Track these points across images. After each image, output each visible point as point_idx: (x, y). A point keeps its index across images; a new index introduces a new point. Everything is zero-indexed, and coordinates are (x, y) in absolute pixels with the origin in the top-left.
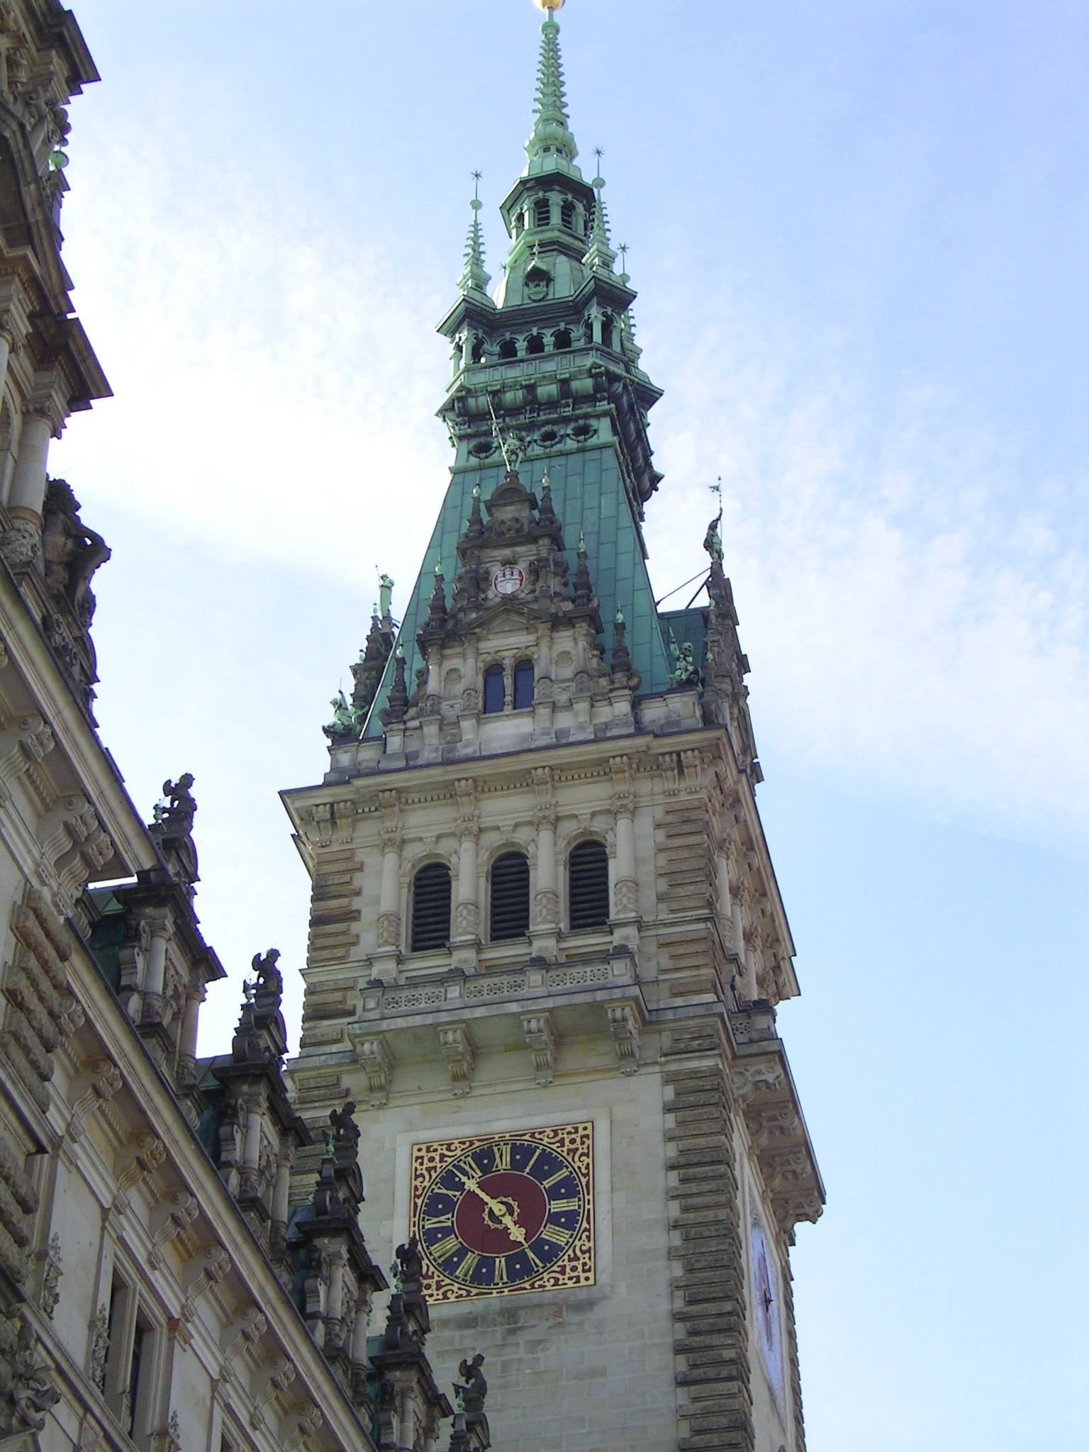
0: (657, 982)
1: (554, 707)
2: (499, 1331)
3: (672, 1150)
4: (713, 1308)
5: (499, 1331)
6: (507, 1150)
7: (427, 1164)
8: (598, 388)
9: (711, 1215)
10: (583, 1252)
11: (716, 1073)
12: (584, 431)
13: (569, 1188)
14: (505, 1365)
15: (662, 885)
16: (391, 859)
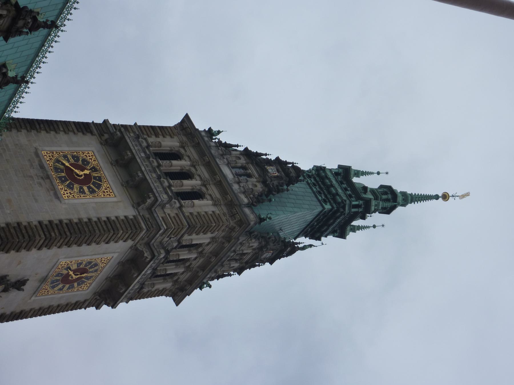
0: (165, 213)
1: (239, 183)
2: (42, 175)
3: (113, 218)
4: (66, 230)
5: (42, 175)
6: (99, 175)
7: (88, 155)
8: (339, 204)
9: (96, 228)
10: (73, 196)
11: (141, 229)
12: (325, 202)
13: (92, 192)
14: (31, 177)
15: (195, 214)
16: (178, 144)
